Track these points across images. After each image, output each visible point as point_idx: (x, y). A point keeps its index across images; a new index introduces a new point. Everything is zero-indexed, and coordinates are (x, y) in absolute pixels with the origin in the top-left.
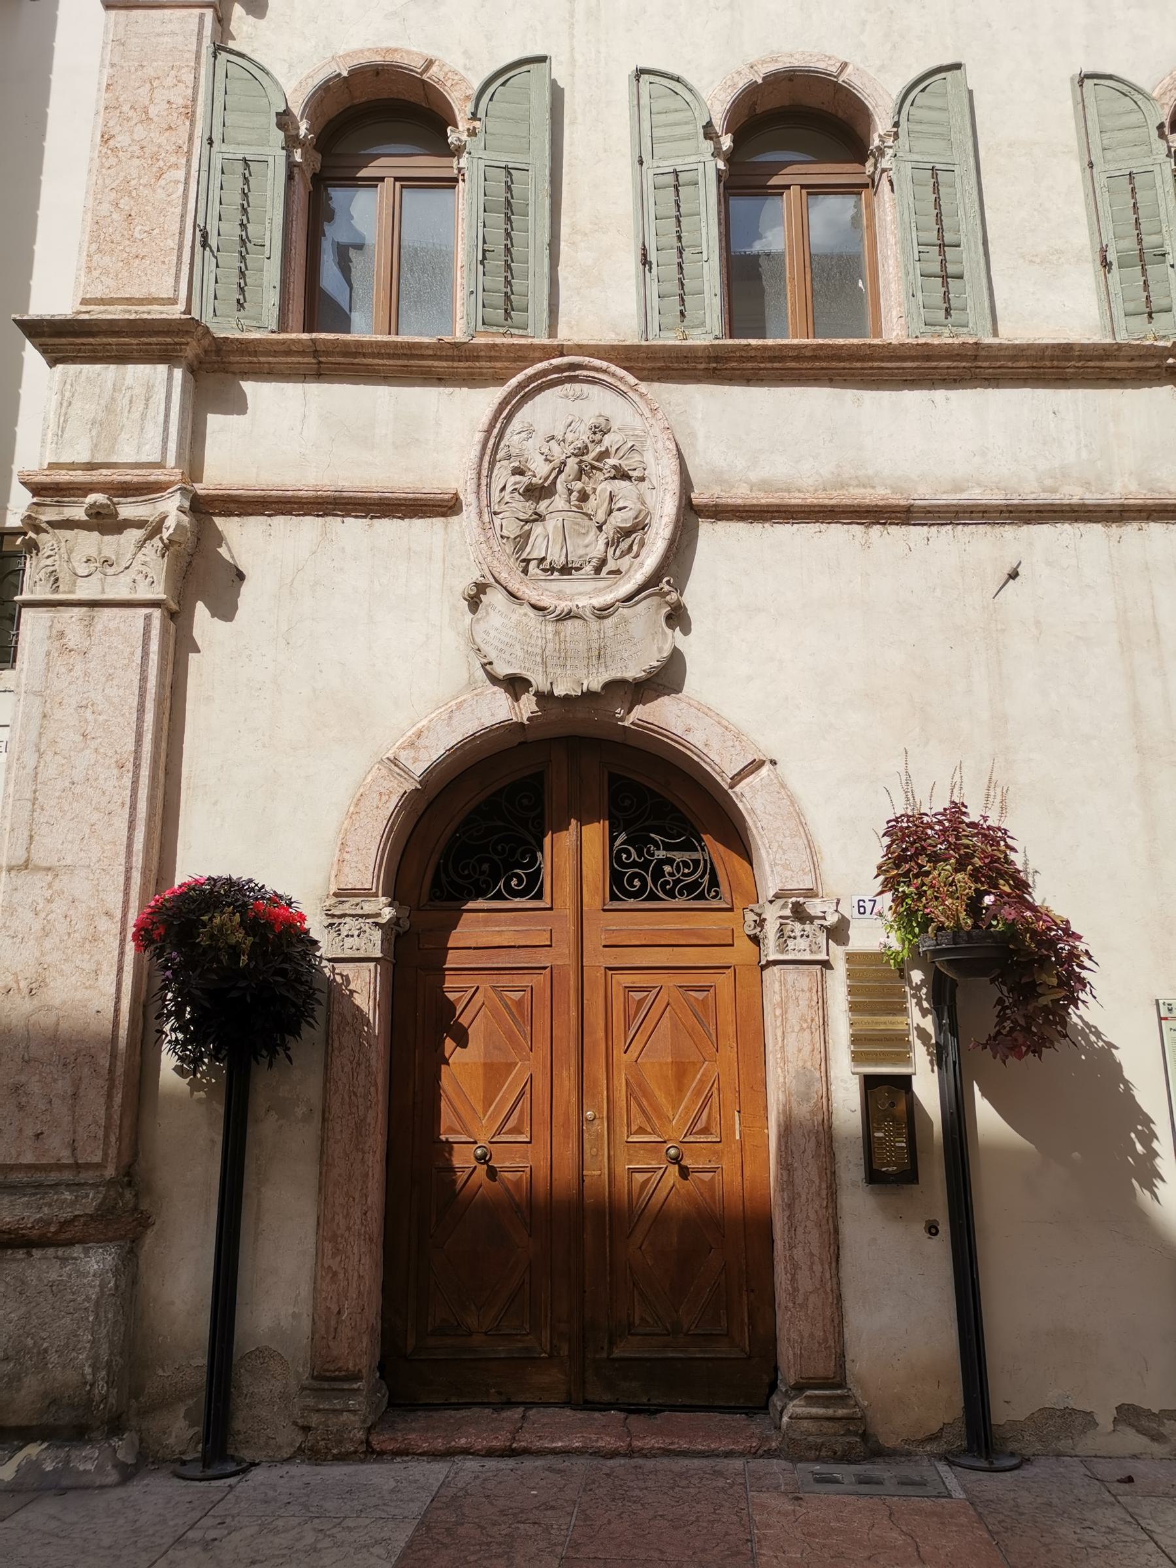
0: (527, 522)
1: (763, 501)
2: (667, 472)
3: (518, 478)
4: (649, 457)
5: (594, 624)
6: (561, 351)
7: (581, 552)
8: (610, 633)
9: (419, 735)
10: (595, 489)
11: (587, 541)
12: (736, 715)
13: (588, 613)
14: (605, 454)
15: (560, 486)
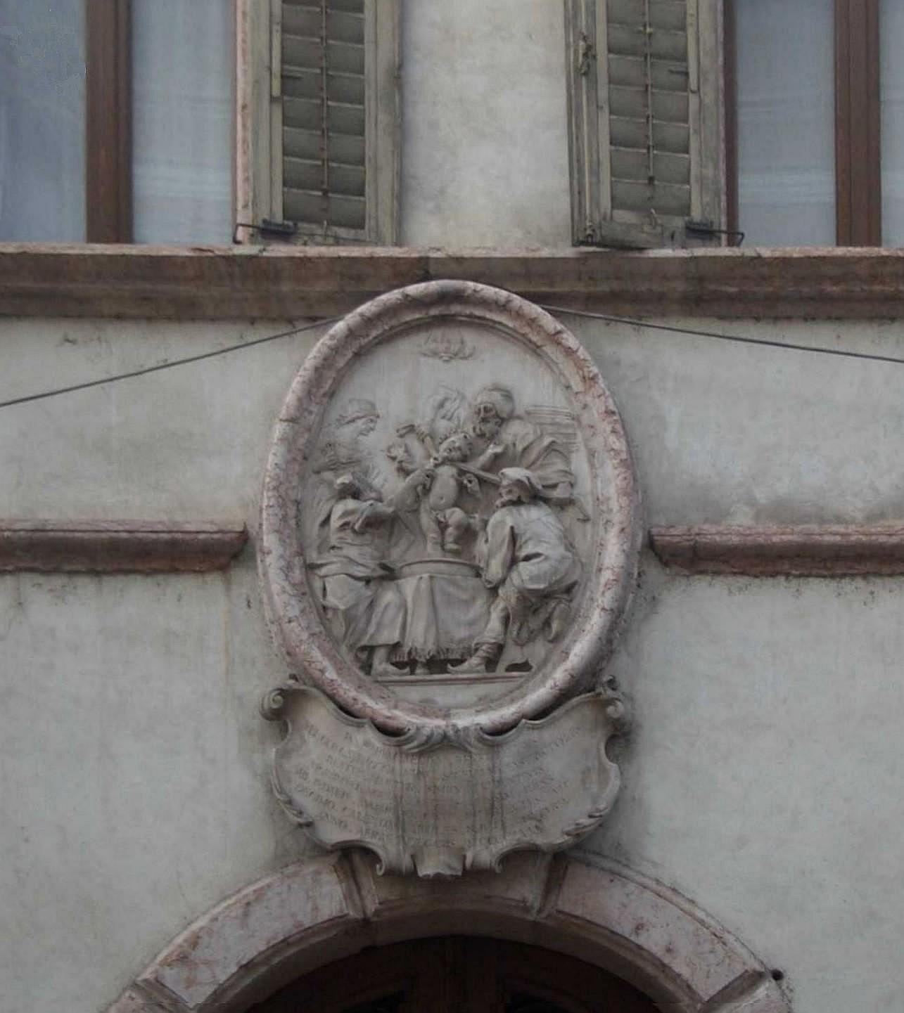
0: (368, 581)
1: (775, 539)
2: (612, 491)
3: (350, 504)
4: (579, 462)
5: (483, 761)
6: (422, 269)
7: (461, 633)
8: (509, 773)
9: (194, 942)
10: (485, 523)
11: (472, 614)
12: (717, 901)
13: (473, 741)
14: (497, 462)
15: (426, 520)
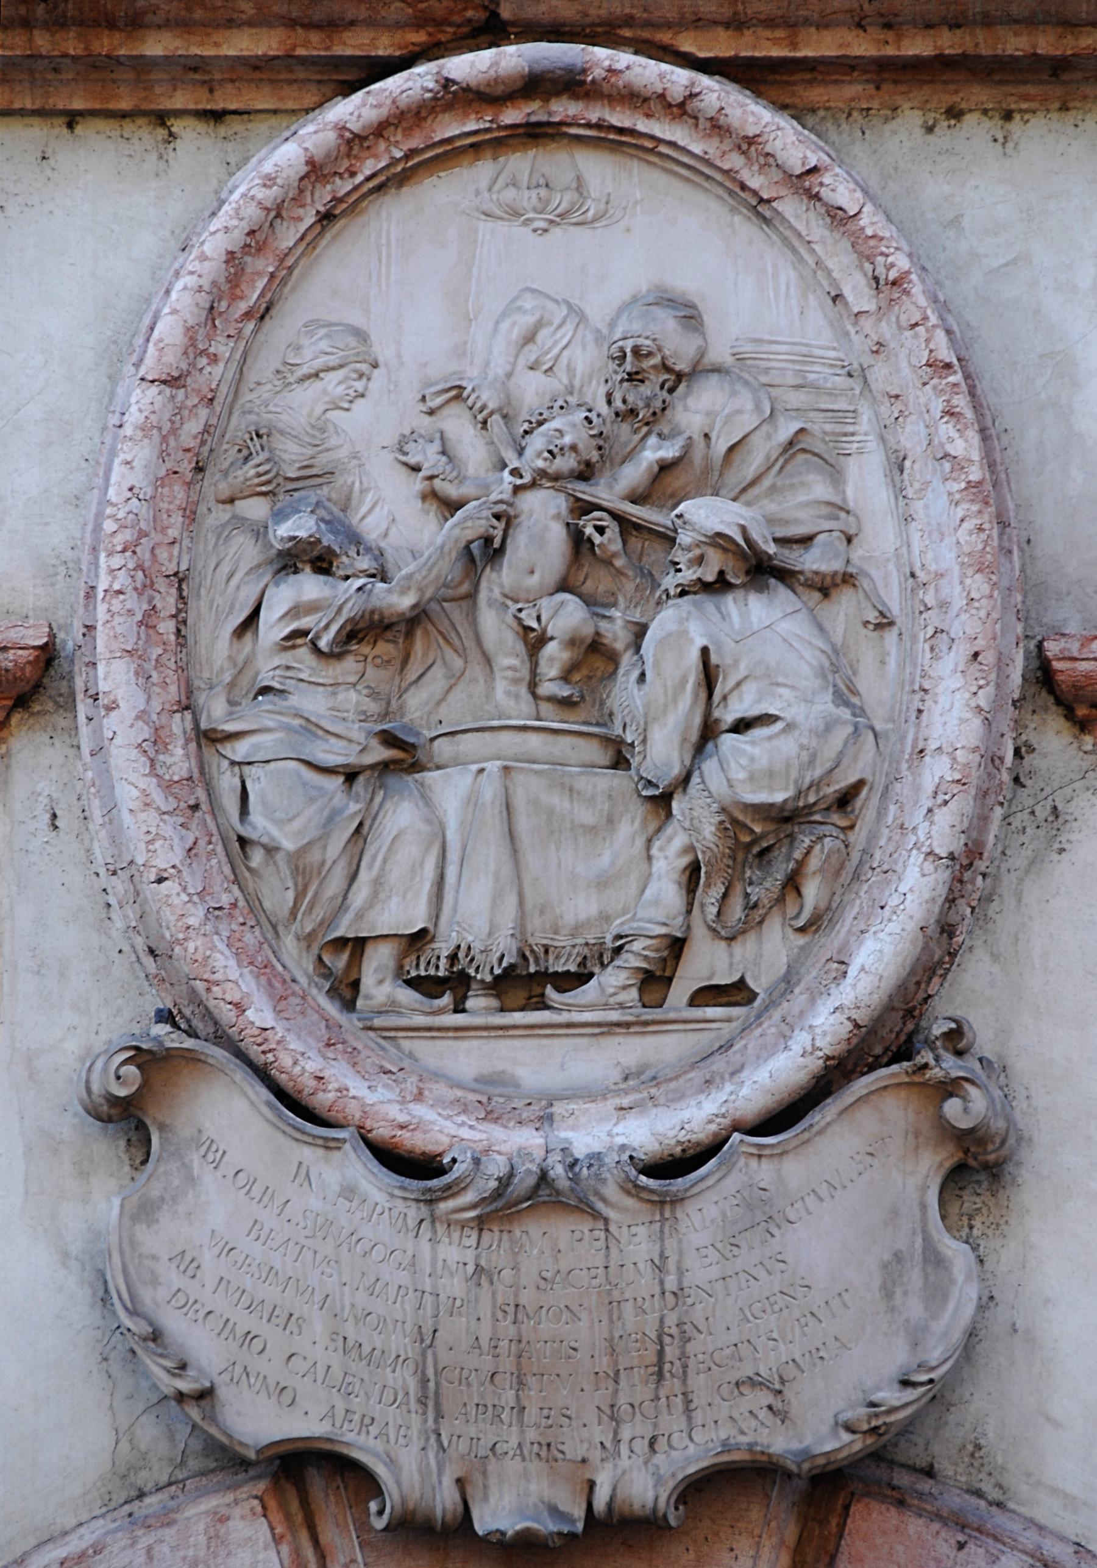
3: (309, 586)
4: (866, 481)
5: (637, 1241)
8: (701, 1272)
10: (640, 631)
